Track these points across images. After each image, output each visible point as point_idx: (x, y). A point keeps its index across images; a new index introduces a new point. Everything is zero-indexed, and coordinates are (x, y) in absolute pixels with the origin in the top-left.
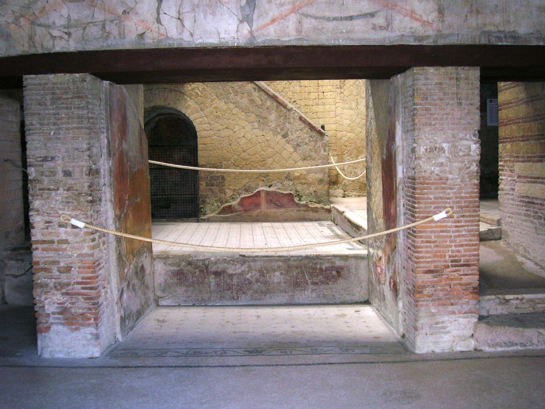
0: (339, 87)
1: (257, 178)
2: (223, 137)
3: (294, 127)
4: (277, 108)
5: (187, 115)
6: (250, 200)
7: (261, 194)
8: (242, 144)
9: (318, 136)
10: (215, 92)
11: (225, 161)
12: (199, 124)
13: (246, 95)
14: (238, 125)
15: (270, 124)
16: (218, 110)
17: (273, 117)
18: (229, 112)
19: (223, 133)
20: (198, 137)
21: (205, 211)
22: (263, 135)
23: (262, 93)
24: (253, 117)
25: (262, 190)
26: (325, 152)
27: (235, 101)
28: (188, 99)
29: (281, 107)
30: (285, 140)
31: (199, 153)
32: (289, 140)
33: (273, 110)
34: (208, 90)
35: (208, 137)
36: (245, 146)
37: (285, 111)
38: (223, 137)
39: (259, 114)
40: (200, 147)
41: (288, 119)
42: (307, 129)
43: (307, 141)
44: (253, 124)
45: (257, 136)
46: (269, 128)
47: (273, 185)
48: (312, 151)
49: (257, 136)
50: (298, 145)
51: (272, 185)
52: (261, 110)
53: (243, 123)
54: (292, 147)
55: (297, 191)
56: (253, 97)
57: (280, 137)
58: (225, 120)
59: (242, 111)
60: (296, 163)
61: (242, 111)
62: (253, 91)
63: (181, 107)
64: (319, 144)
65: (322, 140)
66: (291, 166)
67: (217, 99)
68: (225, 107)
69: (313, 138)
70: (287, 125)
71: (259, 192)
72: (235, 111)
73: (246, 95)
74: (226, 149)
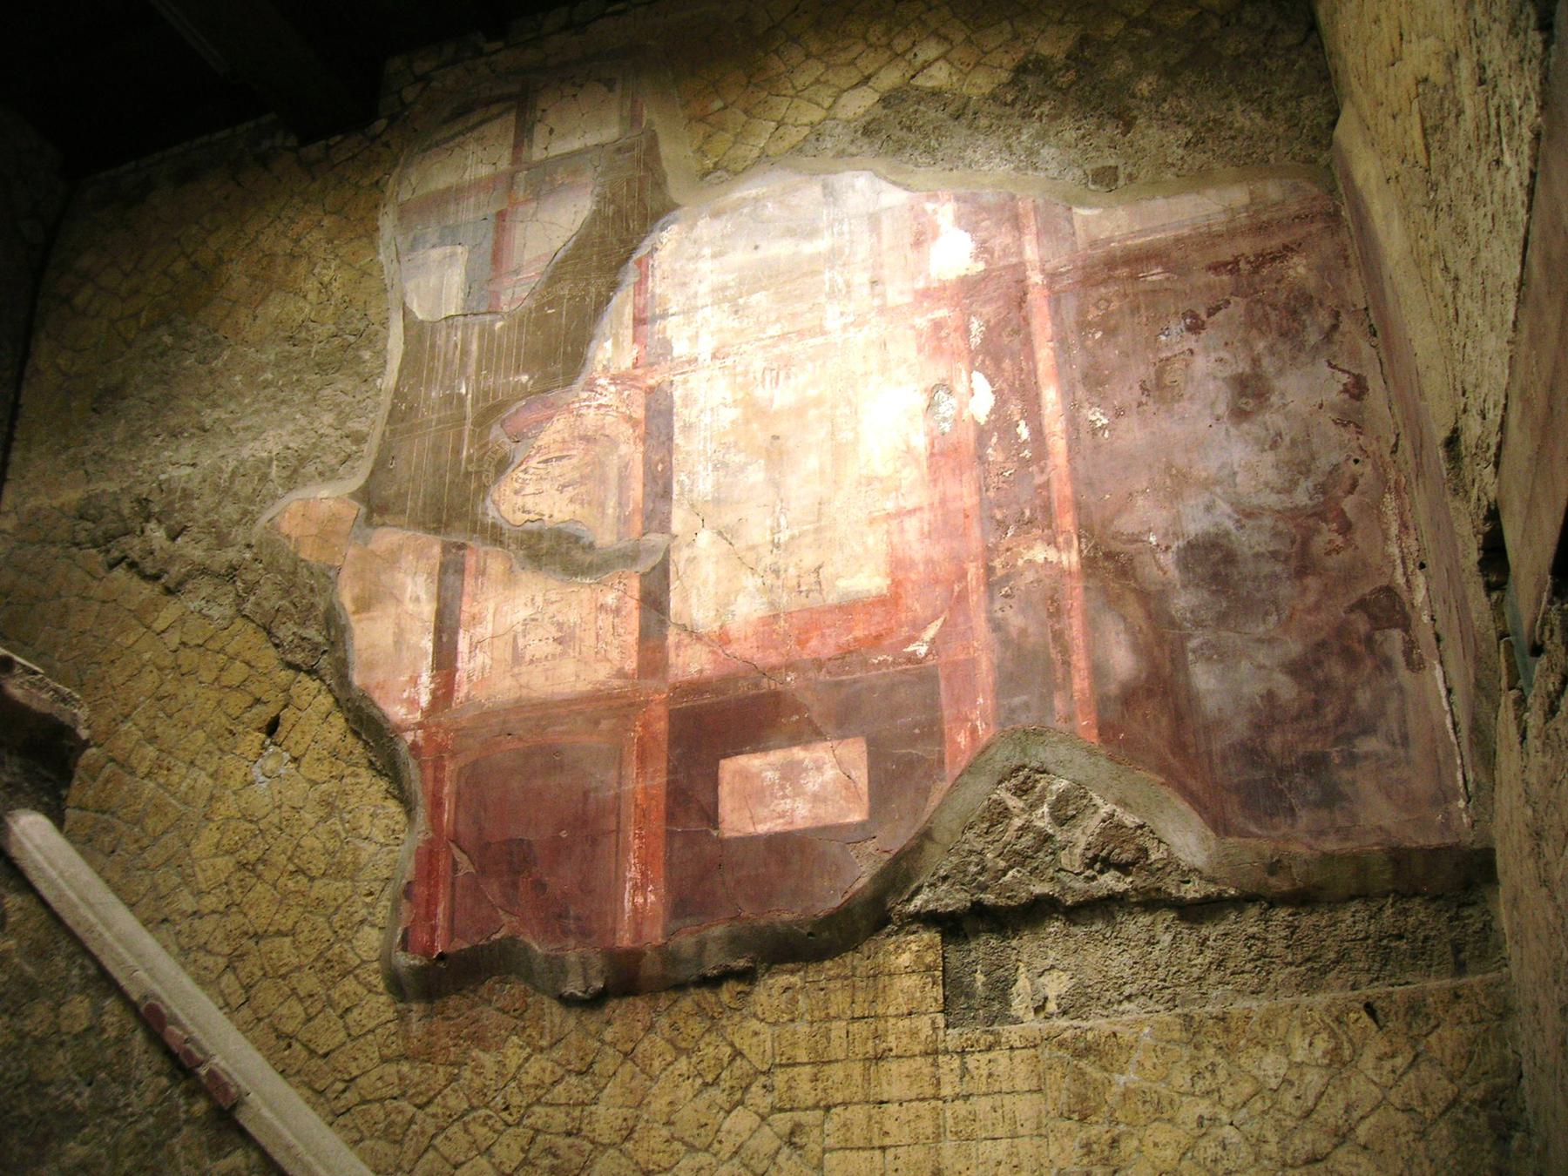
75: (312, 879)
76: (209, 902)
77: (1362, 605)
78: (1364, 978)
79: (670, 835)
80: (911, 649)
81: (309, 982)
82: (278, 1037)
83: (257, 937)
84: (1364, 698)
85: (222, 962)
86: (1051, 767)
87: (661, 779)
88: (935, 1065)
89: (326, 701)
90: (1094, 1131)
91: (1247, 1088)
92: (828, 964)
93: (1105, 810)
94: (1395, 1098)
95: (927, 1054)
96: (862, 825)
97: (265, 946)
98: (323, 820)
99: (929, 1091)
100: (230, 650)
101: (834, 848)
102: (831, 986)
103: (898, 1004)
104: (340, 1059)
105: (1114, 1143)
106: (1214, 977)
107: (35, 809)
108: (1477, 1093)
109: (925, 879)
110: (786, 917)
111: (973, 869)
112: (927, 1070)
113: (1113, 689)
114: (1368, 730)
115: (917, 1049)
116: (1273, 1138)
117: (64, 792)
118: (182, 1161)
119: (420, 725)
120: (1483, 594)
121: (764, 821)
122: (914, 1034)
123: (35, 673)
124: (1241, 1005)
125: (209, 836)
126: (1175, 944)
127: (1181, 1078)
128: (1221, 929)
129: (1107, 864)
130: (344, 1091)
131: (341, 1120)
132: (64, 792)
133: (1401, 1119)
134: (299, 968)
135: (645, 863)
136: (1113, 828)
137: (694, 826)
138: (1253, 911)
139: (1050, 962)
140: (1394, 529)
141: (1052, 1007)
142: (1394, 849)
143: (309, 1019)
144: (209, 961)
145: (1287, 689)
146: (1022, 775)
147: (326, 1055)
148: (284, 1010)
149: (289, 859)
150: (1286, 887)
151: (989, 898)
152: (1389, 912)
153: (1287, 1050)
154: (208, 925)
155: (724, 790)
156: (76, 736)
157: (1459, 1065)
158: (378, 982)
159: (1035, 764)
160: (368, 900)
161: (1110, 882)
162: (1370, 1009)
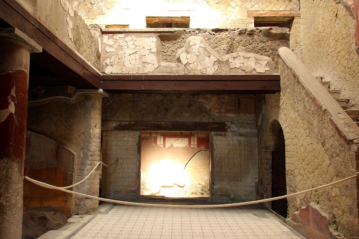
11: (296, 169)
17: (315, 123)
22: (312, 144)
26: (353, 167)
32: (326, 149)
39: (309, 121)
53: (302, 131)
54: (328, 158)
70: (324, 130)
75: (345, 39)
76: (333, 49)
81: (347, 57)
82: (344, 67)
83: (339, 52)
85: (336, 58)
89: (342, 7)
97: (341, 53)
98: (345, 28)
100: (329, 5)
104: (352, 68)
107: (283, 46)
117: (288, 42)
119: (354, 4)
123: (277, 28)
125: (331, 38)
130: (353, 73)
131: (354, 78)
132: (288, 42)
134: (345, 55)
143: (348, 63)
144: (334, 59)
147: (350, 68)
148: (344, 63)
149: (342, 37)
154: (333, 53)
156: (287, 34)
158: (355, 53)
160: (353, 39)
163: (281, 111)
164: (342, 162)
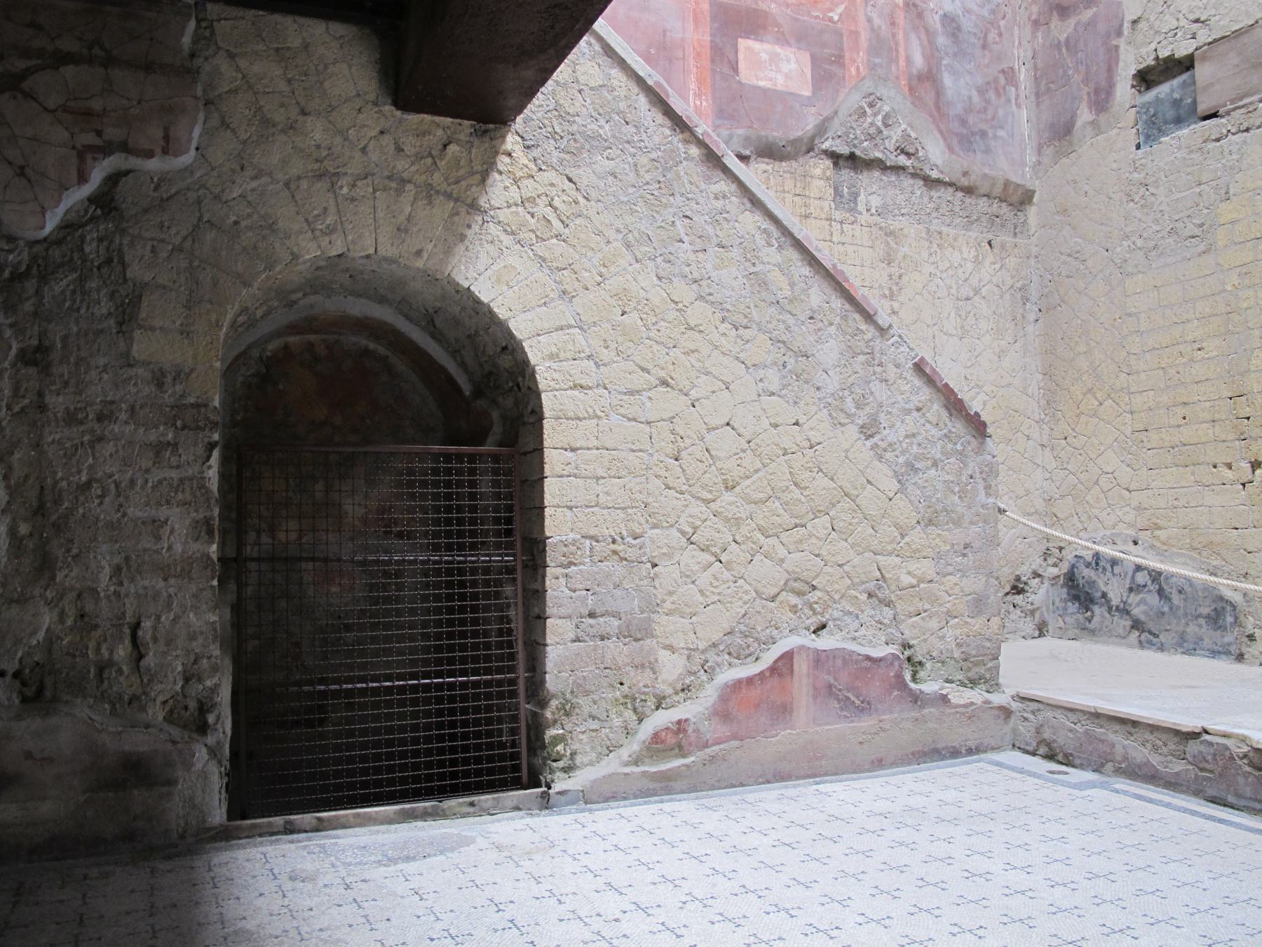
0: (887, 292)
1: (773, 599)
2: (648, 423)
3: (899, 398)
4: (845, 318)
5: (501, 312)
6: (755, 692)
7: (796, 667)
8: (721, 454)
9: (969, 438)
10: (619, 224)
11: (655, 526)
12: (552, 357)
13: (735, 253)
14: (707, 373)
15: (820, 378)
16: (633, 304)
17: (829, 351)
18: (672, 315)
19: (648, 404)
20: (547, 412)
21: (573, 754)
22: (797, 424)
23: (794, 255)
24: (760, 349)
25: (802, 647)
26: (988, 495)
27: (696, 275)
28: (507, 240)
29: (857, 316)
30: (869, 443)
31: (553, 490)
32: (883, 445)
33: (831, 324)
34: (592, 213)
35: (590, 418)
36: (732, 463)
37: (869, 336)
38: (648, 423)
39: (784, 338)
40: (553, 459)
41: (880, 365)
42: (936, 409)
43: (936, 452)
44: (761, 373)
45: (776, 426)
46: (819, 394)
47: (831, 624)
48: (952, 492)
49: (776, 426)
50: (911, 467)
51: (824, 627)
52: (790, 321)
54: (891, 473)
55: (906, 646)
56: (759, 267)
57: (852, 431)
58: (655, 347)
59: (723, 320)
60: (903, 536)
61: (723, 320)
62: (760, 240)
63: (472, 274)
64: (972, 467)
65: (980, 450)
66: (889, 548)
67: (630, 258)
68: (657, 296)
69: (955, 444)
70: (876, 386)
71: (788, 657)
72: (699, 313)
73: (735, 253)
74: (663, 473)
77: (1003, 71)
78: (985, 230)
79: (714, 71)
80: (831, 14)
84: (1001, 112)
86: (884, 98)
87: (708, 38)
88: (830, 225)
90: (893, 270)
91: (948, 265)
92: (784, 164)
93: (904, 126)
94: (995, 280)
95: (827, 219)
96: (809, 98)
99: (828, 238)
101: (797, 106)
102: (785, 175)
103: (814, 193)
105: (900, 277)
106: (934, 215)
108: (1019, 285)
109: (829, 134)
110: (775, 134)
111: (852, 136)
112: (827, 227)
113: (915, 71)
114: (1001, 127)
115: (823, 216)
116: (955, 287)
118: (686, 181)
120: (1129, 87)
121: (761, 80)
122: (822, 209)
124: (945, 229)
126: (921, 197)
127: (925, 255)
128: (939, 194)
129: (903, 152)
133: (996, 289)
135: (700, 82)
136: (906, 136)
137: (726, 70)
138: (951, 190)
139: (874, 190)
140: (1016, 43)
141: (873, 211)
142: (1007, 180)
145: (976, 98)
146: (872, 98)
150: (966, 184)
151: (858, 153)
152: (995, 205)
153: (961, 252)
155: (741, 56)
157: (1014, 273)
159: (878, 95)
161: (903, 160)
162: (990, 243)
163: (493, 229)
164: (952, 482)
